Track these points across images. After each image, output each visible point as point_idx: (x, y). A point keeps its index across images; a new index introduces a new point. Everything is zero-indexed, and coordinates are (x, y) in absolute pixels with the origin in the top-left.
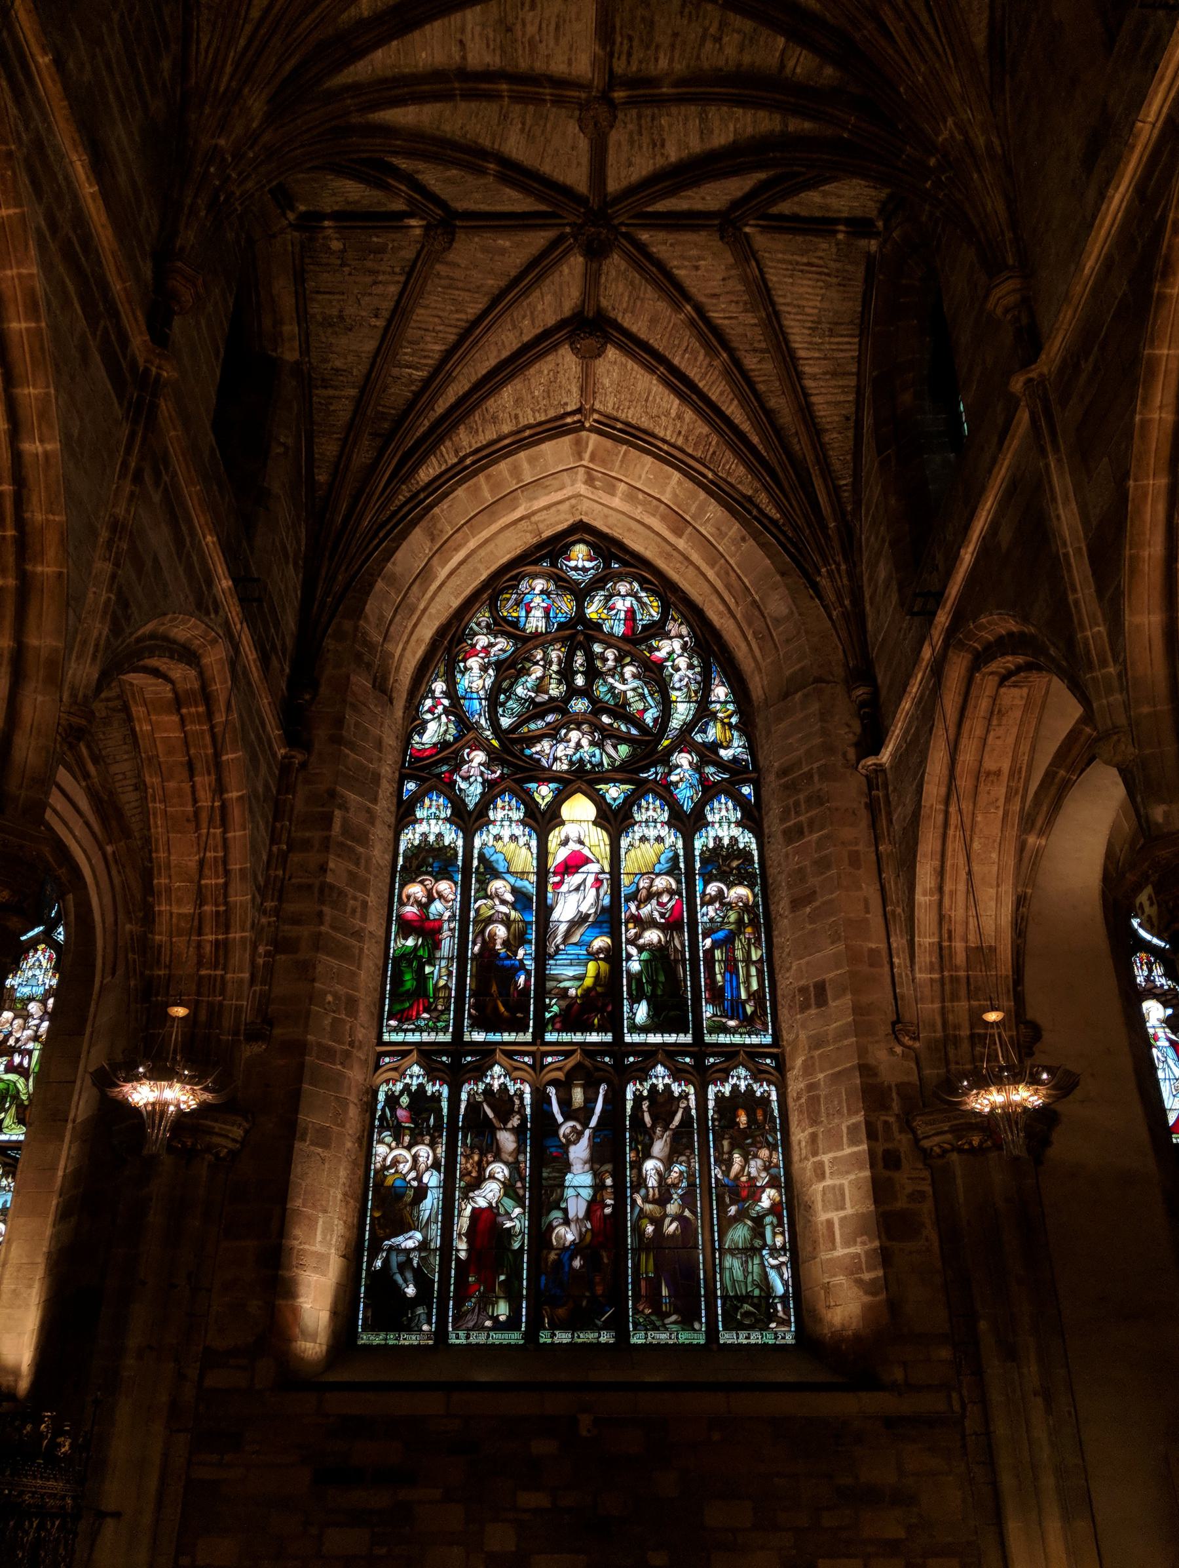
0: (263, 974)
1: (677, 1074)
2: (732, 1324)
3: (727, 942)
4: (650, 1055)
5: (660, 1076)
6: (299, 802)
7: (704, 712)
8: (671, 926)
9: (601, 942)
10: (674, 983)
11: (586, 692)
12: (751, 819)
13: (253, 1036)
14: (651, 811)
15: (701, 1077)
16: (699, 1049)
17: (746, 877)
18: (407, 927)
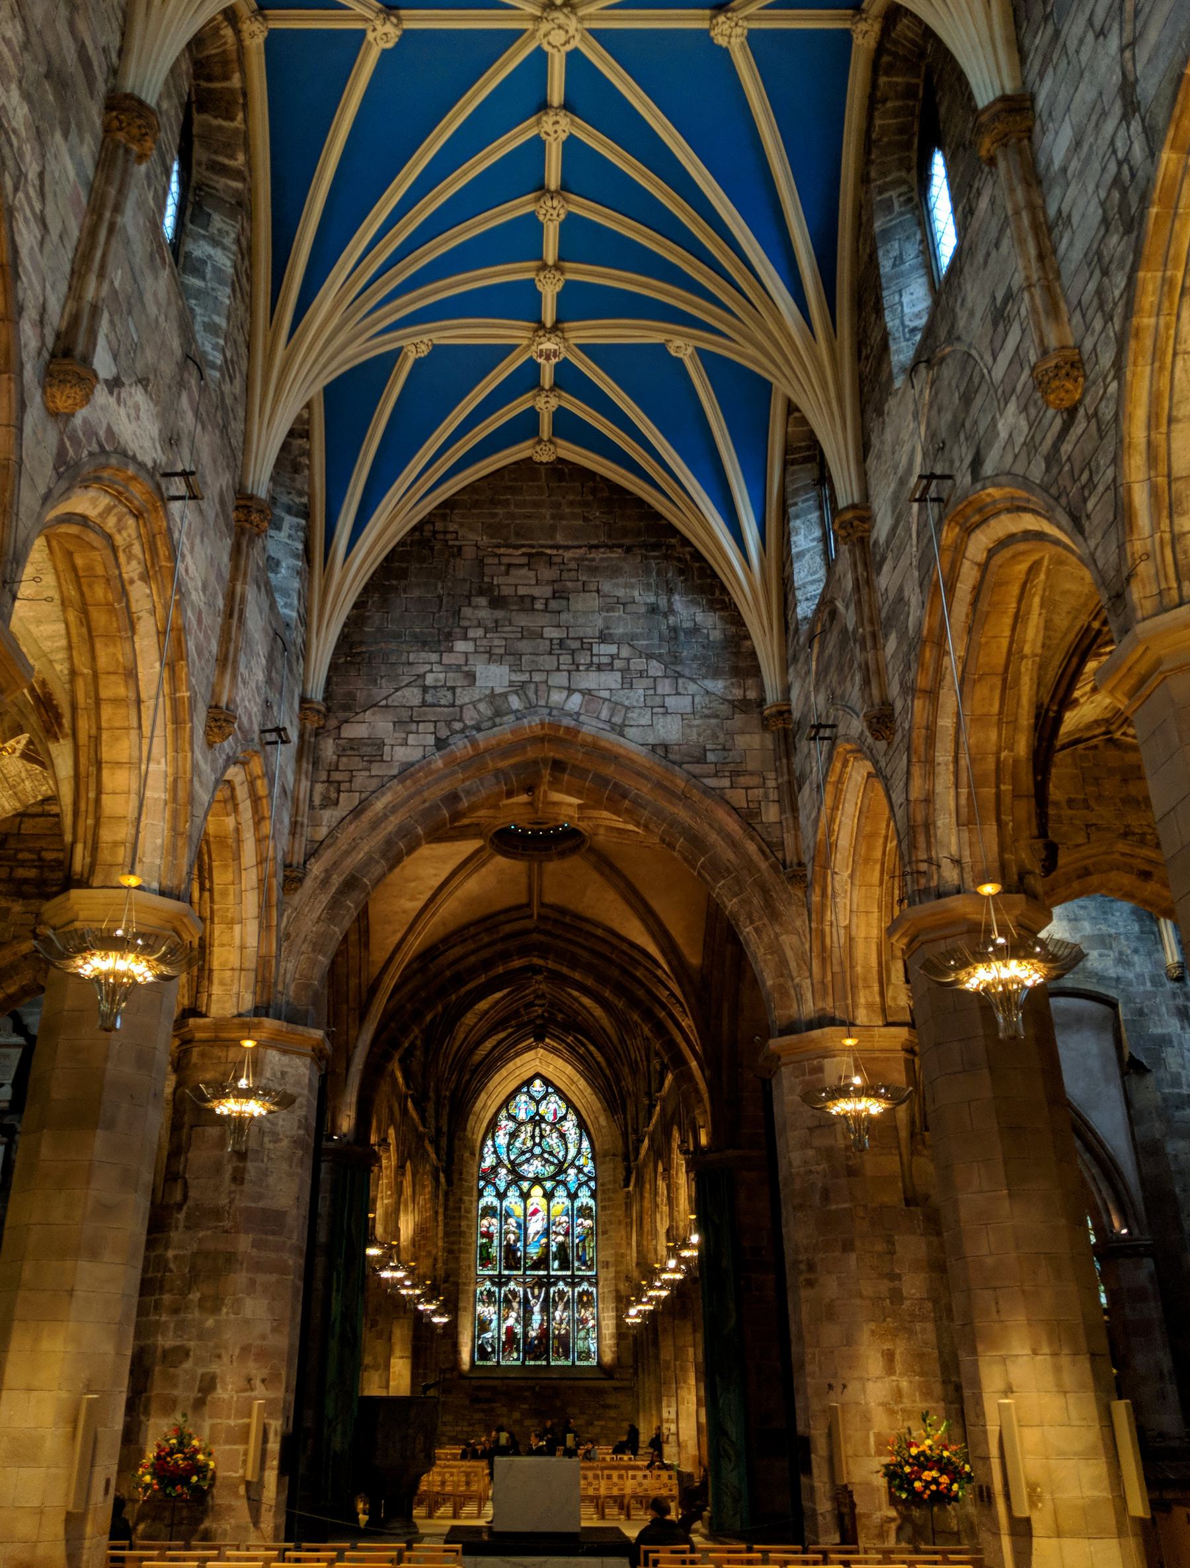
0: (446, 1262)
1: (566, 1284)
2: (579, 1359)
3: (583, 1241)
4: (558, 1278)
5: (561, 1285)
6: (451, 1204)
7: (579, 1152)
8: (566, 1234)
9: (544, 1240)
10: (566, 1255)
11: (540, 1145)
12: (593, 1195)
13: (445, 1282)
14: (561, 1192)
15: (573, 1285)
16: (573, 1276)
17: (590, 1217)
18: (484, 1235)
